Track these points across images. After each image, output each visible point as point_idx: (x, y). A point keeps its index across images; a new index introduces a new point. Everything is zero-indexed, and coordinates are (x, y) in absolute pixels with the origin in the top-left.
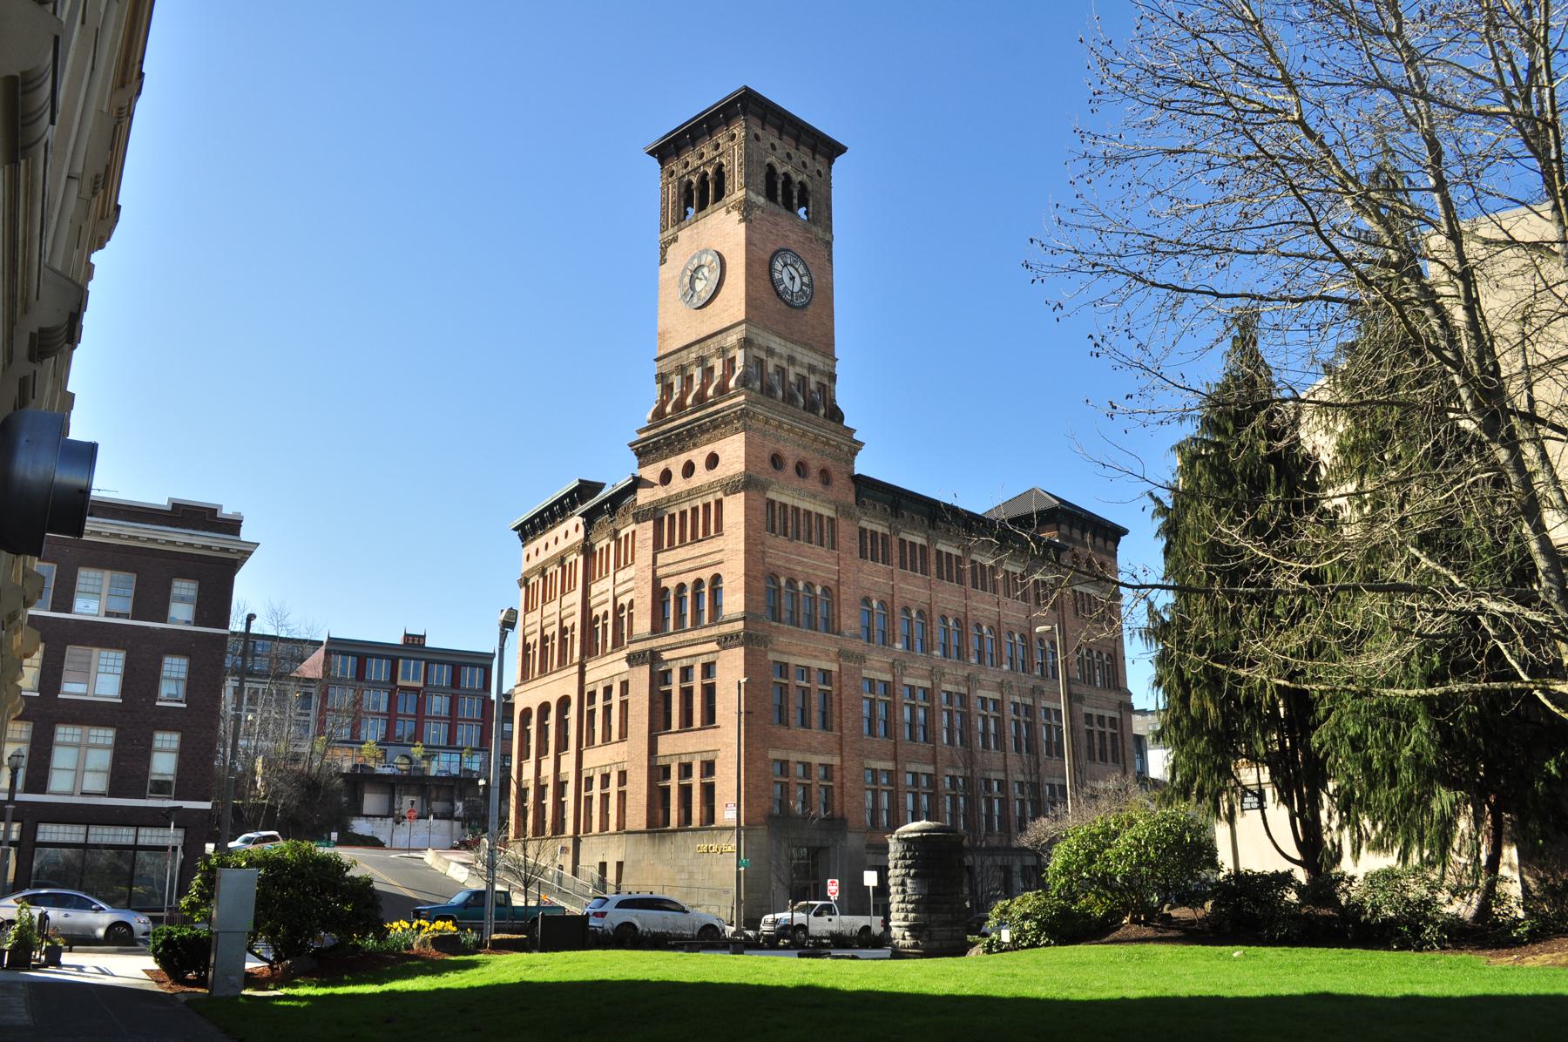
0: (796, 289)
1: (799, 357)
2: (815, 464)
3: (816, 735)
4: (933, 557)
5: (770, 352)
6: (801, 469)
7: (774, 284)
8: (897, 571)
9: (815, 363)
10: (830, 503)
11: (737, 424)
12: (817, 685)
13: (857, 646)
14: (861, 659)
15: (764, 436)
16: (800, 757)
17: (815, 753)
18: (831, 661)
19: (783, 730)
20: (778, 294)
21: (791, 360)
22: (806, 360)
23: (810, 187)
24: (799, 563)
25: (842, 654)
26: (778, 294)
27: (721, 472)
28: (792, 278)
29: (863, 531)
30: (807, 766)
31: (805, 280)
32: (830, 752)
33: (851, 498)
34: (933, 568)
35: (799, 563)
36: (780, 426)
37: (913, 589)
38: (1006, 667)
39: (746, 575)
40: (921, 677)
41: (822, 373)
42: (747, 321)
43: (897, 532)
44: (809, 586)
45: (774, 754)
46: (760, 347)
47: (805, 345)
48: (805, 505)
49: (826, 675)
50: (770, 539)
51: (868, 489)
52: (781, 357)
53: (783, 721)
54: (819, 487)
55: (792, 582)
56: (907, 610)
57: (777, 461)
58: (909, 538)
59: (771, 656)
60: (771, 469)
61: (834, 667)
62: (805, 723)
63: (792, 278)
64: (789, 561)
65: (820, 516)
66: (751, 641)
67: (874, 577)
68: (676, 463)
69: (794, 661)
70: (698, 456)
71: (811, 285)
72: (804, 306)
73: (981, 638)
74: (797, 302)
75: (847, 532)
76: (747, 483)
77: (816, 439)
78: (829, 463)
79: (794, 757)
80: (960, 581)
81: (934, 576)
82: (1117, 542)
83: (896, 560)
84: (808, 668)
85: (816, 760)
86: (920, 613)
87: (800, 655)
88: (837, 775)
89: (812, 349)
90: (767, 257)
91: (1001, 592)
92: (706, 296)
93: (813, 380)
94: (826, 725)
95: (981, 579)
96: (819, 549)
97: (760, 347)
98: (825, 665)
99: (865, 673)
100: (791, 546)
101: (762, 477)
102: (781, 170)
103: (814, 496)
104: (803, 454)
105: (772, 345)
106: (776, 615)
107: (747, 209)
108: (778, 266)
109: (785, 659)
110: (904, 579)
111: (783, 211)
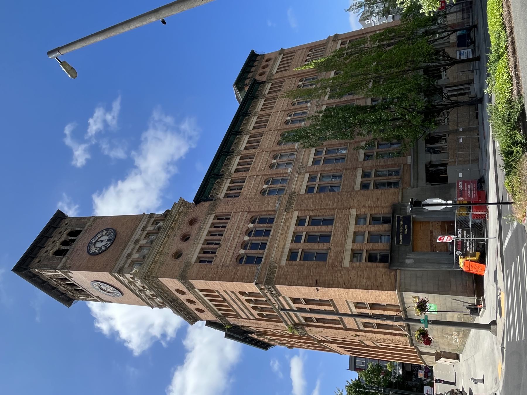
0: (105, 238)
1: (137, 237)
2: (185, 229)
3: (335, 229)
4: (247, 152)
5: (129, 256)
6: (186, 238)
7: (102, 252)
8: (250, 173)
9: (142, 226)
10: (206, 218)
11: (155, 280)
12: (306, 229)
13: (285, 197)
14: (293, 194)
15: (162, 263)
16: (350, 240)
17: (347, 228)
18: (292, 217)
19: (331, 254)
20: (106, 250)
21: (137, 242)
22: (139, 232)
23: (70, 230)
24: (234, 239)
25: (287, 209)
26: (106, 250)
27: (183, 288)
28: (102, 241)
29: (227, 196)
30: (356, 234)
31: (99, 236)
32: (348, 216)
33: (207, 204)
34: (252, 151)
35: (234, 239)
36: (160, 253)
37: (261, 162)
38: (309, 104)
39: (232, 281)
40: (309, 155)
41: (148, 222)
42: (110, 273)
43: (230, 173)
44: (249, 233)
45: (347, 263)
46: (125, 263)
47: (132, 234)
48: (204, 235)
49: (300, 222)
50: (217, 261)
51: (204, 194)
52: (133, 249)
53: (322, 256)
54: (197, 225)
55: (244, 246)
56: (272, 166)
57: (178, 255)
58: (235, 167)
59: (284, 262)
60: (180, 259)
61: (296, 214)
62: (325, 238)
63: (102, 241)
64: (231, 247)
65: (213, 225)
66: (269, 281)
67: (251, 187)
68: (192, 307)
69: (288, 245)
70: (182, 298)
71: (107, 230)
72: (116, 234)
73: (293, 121)
74: (112, 237)
75: (221, 209)
76: (183, 278)
77: (172, 228)
78: (187, 219)
79: (349, 245)
80: (261, 135)
81: (257, 150)
82: (257, 55)
83: (244, 174)
84: (294, 233)
85: (352, 228)
86: (275, 157)
87: (285, 240)
88: (363, 211)
89: (135, 230)
90: (89, 256)
91: (270, 111)
92: (112, 288)
93: (150, 228)
94: (329, 222)
95: (261, 124)
96: (228, 226)
97: (125, 263)
98: (294, 221)
99: (303, 191)
100: (223, 246)
101: (183, 266)
102: (55, 249)
103: (200, 229)
104: (178, 238)
105: (126, 255)
106: (259, 260)
107: (66, 268)
108: (93, 250)
109: (286, 251)
110: (254, 168)
111: (73, 246)
